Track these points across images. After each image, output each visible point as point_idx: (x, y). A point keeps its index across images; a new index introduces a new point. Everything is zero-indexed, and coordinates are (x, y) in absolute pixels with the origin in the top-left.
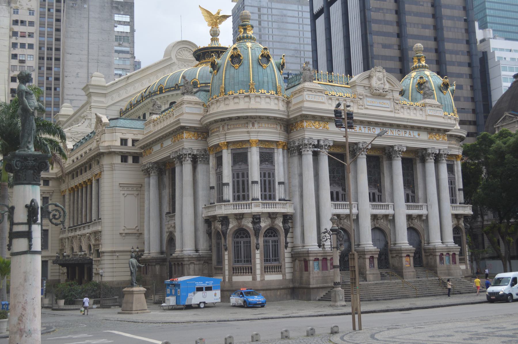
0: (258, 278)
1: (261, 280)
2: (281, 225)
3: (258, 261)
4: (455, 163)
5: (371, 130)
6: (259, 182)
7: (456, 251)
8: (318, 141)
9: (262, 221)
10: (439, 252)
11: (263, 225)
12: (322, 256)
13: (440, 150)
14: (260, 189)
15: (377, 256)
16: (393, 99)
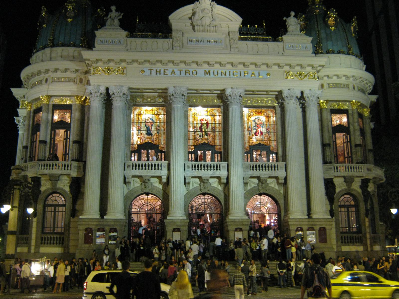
0: (33, 251)
1: (35, 253)
2: (67, 189)
3: (34, 230)
4: (350, 112)
5: (191, 73)
6: (48, 141)
7: (326, 225)
8: (107, 89)
9: (42, 184)
10: (294, 225)
11: (43, 189)
12: (97, 225)
13: (302, 93)
14: (48, 149)
15: (186, 228)
16: (229, 35)
